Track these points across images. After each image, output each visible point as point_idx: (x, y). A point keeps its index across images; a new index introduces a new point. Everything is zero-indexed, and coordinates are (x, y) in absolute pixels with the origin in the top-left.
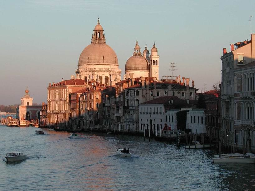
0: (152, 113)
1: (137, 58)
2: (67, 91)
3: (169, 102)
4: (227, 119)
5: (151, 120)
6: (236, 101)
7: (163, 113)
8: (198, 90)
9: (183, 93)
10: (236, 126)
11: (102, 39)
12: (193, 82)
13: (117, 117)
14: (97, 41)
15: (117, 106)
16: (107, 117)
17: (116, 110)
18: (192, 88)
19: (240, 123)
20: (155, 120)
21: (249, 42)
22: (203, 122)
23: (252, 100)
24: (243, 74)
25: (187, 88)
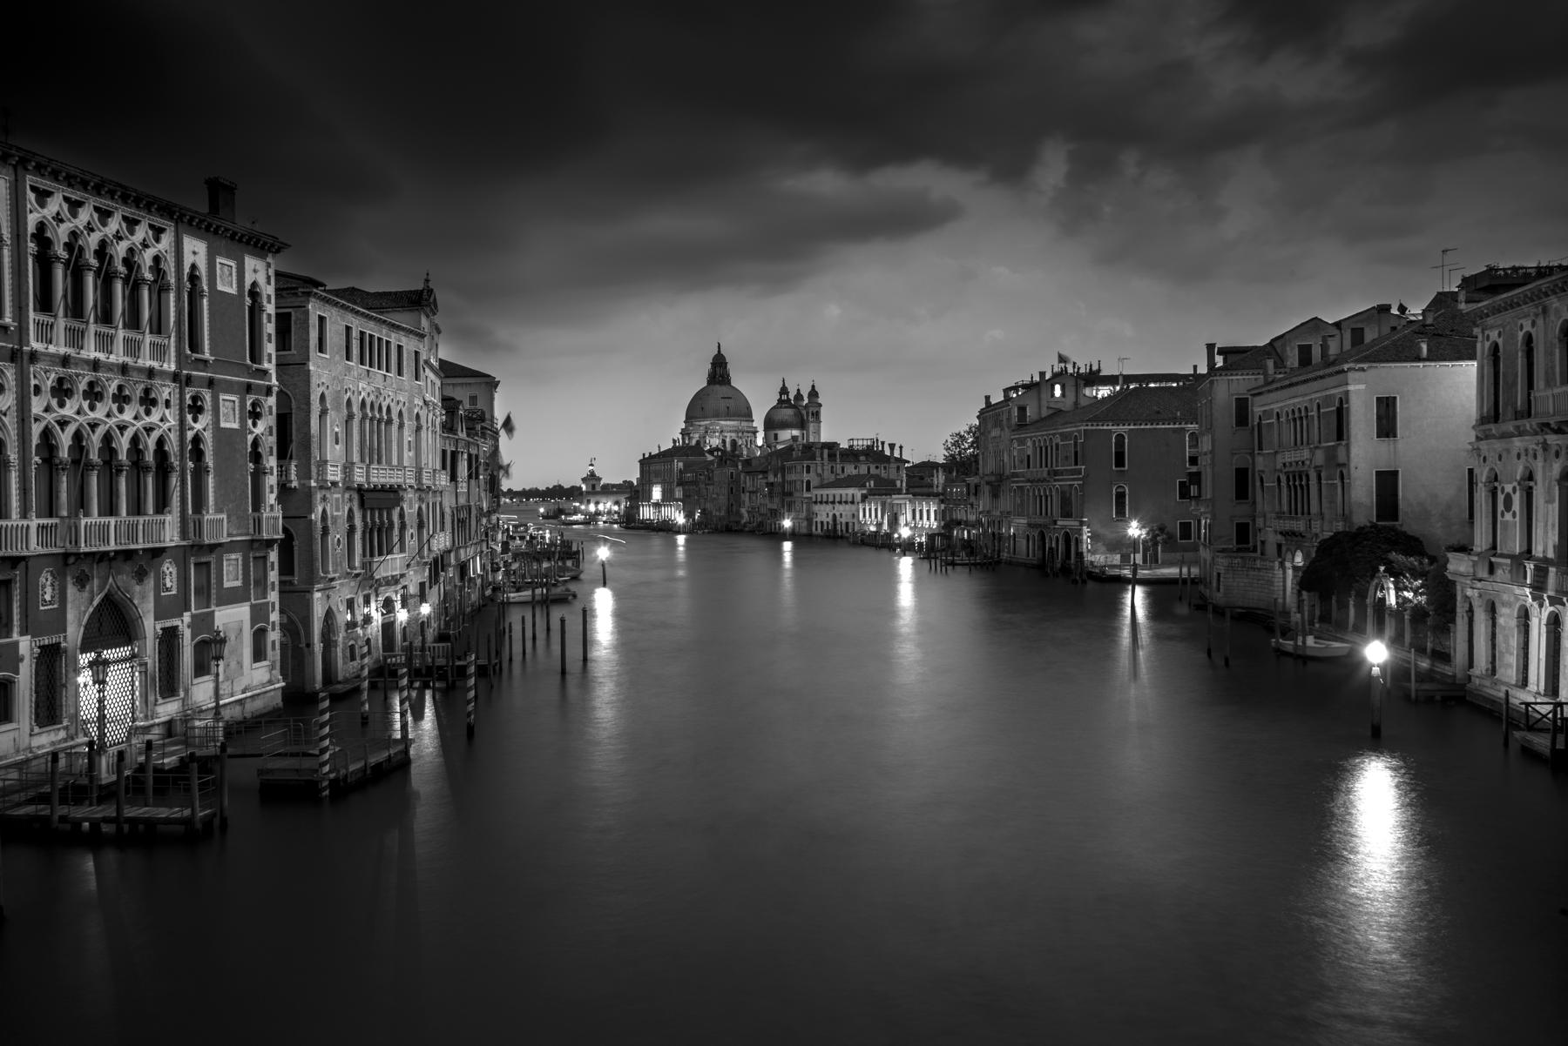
1: (785, 407)
3: (868, 484)
5: (834, 515)
8: (908, 462)
9: (885, 468)
12: (901, 447)
13: (771, 510)
15: (771, 493)
18: (901, 461)
19: (1025, 521)
20: (841, 514)
21: (1037, 384)
25: (892, 460)
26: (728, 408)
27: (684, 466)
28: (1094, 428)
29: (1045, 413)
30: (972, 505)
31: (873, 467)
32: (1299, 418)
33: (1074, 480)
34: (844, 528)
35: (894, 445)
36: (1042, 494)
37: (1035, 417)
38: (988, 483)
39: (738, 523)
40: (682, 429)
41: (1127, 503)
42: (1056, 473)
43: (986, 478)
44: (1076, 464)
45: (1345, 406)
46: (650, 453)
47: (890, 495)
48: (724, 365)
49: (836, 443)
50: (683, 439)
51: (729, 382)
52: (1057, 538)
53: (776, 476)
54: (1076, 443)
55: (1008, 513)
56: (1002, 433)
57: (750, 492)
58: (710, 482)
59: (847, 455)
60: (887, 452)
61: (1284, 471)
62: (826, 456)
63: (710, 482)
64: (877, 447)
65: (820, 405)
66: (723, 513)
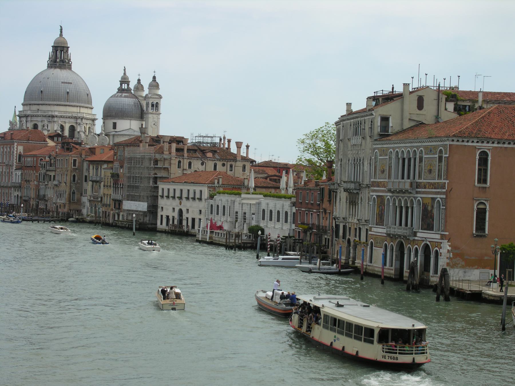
0: (184, 199)
1: (125, 97)
2: (15, 149)
3: (216, 181)
4: (350, 221)
5: (181, 212)
6: (374, 194)
7: (205, 200)
9: (231, 166)
10: (373, 235)
11: (67, 61)
12: (248, 147)
13: (115, 200)
14: (58, 64)
15: (116, 183)
16: (92, 199)
17: (112, 188)
19: (384, 231)
21: (400, 95)
22: (289, 221)
24: (394, 151)
25: (239, 158)
26: (68, 92)
27: (24, 150)
29: (407, 125)
30: (325, 210)
31: (219, 164)
34: (190, 224)
35: (241, 143)
36: (403, 205)
37: (397, 128)
38: (345, 190)
39: (79, 212)
40: (19, 111)
41: (487, 219)
42: (418, 185)
43: (345, 185)
44: (440, 177)
47: (239, 194)
48: (65, 49)
49: (183, 138)
50: (20, 121)
51: (69, 67)
52: (416, 249)
53: (122, 167)
54: (440, 158)
55: (366, 221)
56: (363, 142)
57: (93, 181)
58: (51, 168)
59: (195, 151)
60: (234, 149)
62: (173, 150)
63: (51, 168)
65: (160, 97)
66: (63, 201)
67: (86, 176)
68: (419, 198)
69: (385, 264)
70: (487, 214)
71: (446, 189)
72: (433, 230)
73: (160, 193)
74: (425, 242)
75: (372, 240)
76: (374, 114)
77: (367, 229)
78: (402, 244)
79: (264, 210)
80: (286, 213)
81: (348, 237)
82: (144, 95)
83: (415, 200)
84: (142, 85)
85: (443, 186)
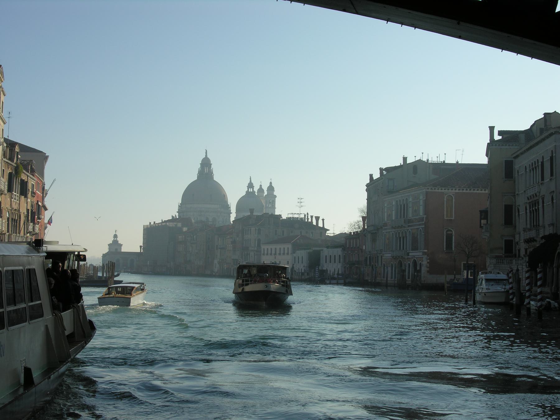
6: (385, 231)
9: (312, 233)
12: (323, 220)
19: (390, 255)
22: (341, 261)
23: (405, 228)
28: (434, 190)
32: (533, 168)
33: (420, 225)
36: (401, 236)
42: (410, 221)
45: (554, 155)
46: (154, 222)
52: (409, 264)
55: (380, 250)
60: (314, 223)
61: (528, 201)
64: (308, 219)
65: (275, 196)
67: (217, 246)
68: (410, 230)
69: (392, 278)
70: (453, 237)
71: (425, 221)
72: (418, 250)
73: (262, 252)
74: (414, 259)
75: (384, 263)
76: (383, 178)
77: (381, 256)
78: (401, 261)
79: (326, 256)
80: (340, 255)
81: (372, 264)
82: (264, 196)
83: (408, 231)
84: (263, 190)
85: (422, 219)
